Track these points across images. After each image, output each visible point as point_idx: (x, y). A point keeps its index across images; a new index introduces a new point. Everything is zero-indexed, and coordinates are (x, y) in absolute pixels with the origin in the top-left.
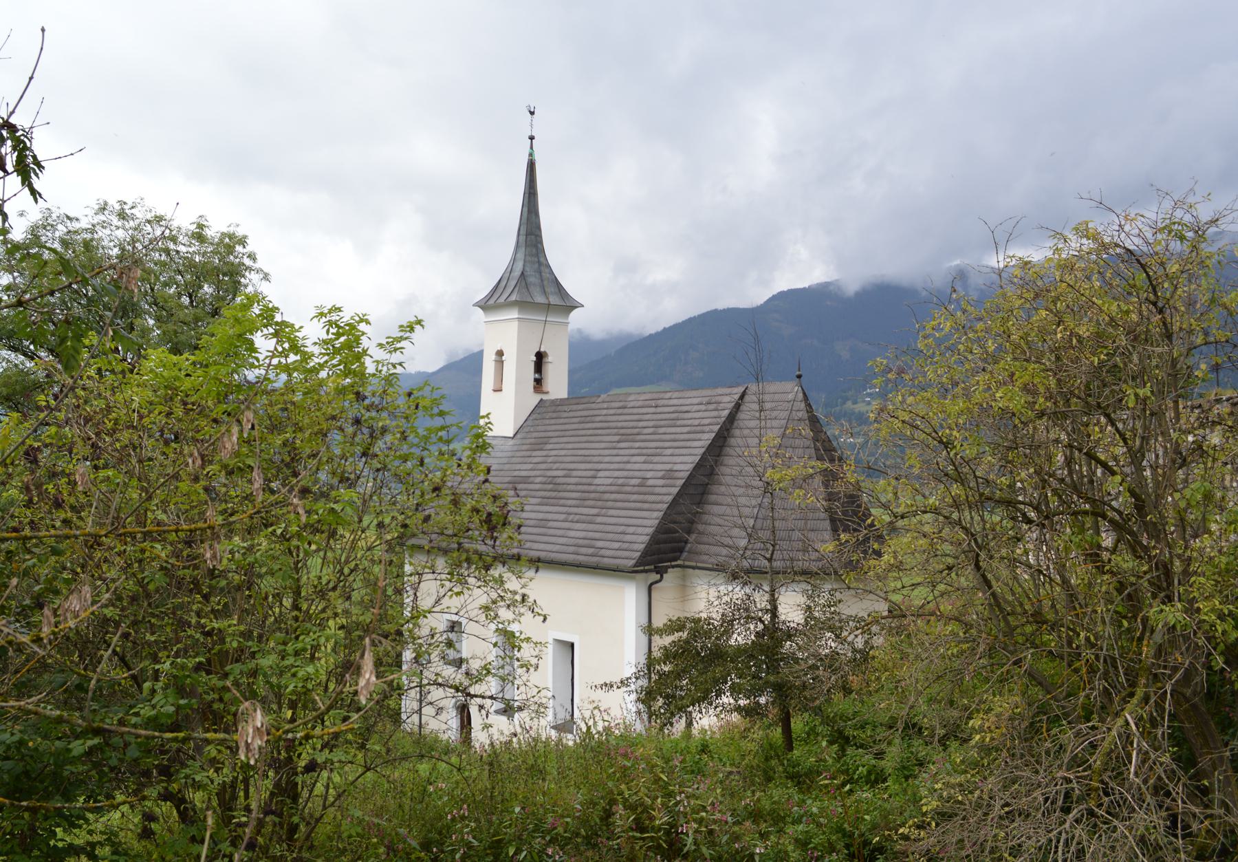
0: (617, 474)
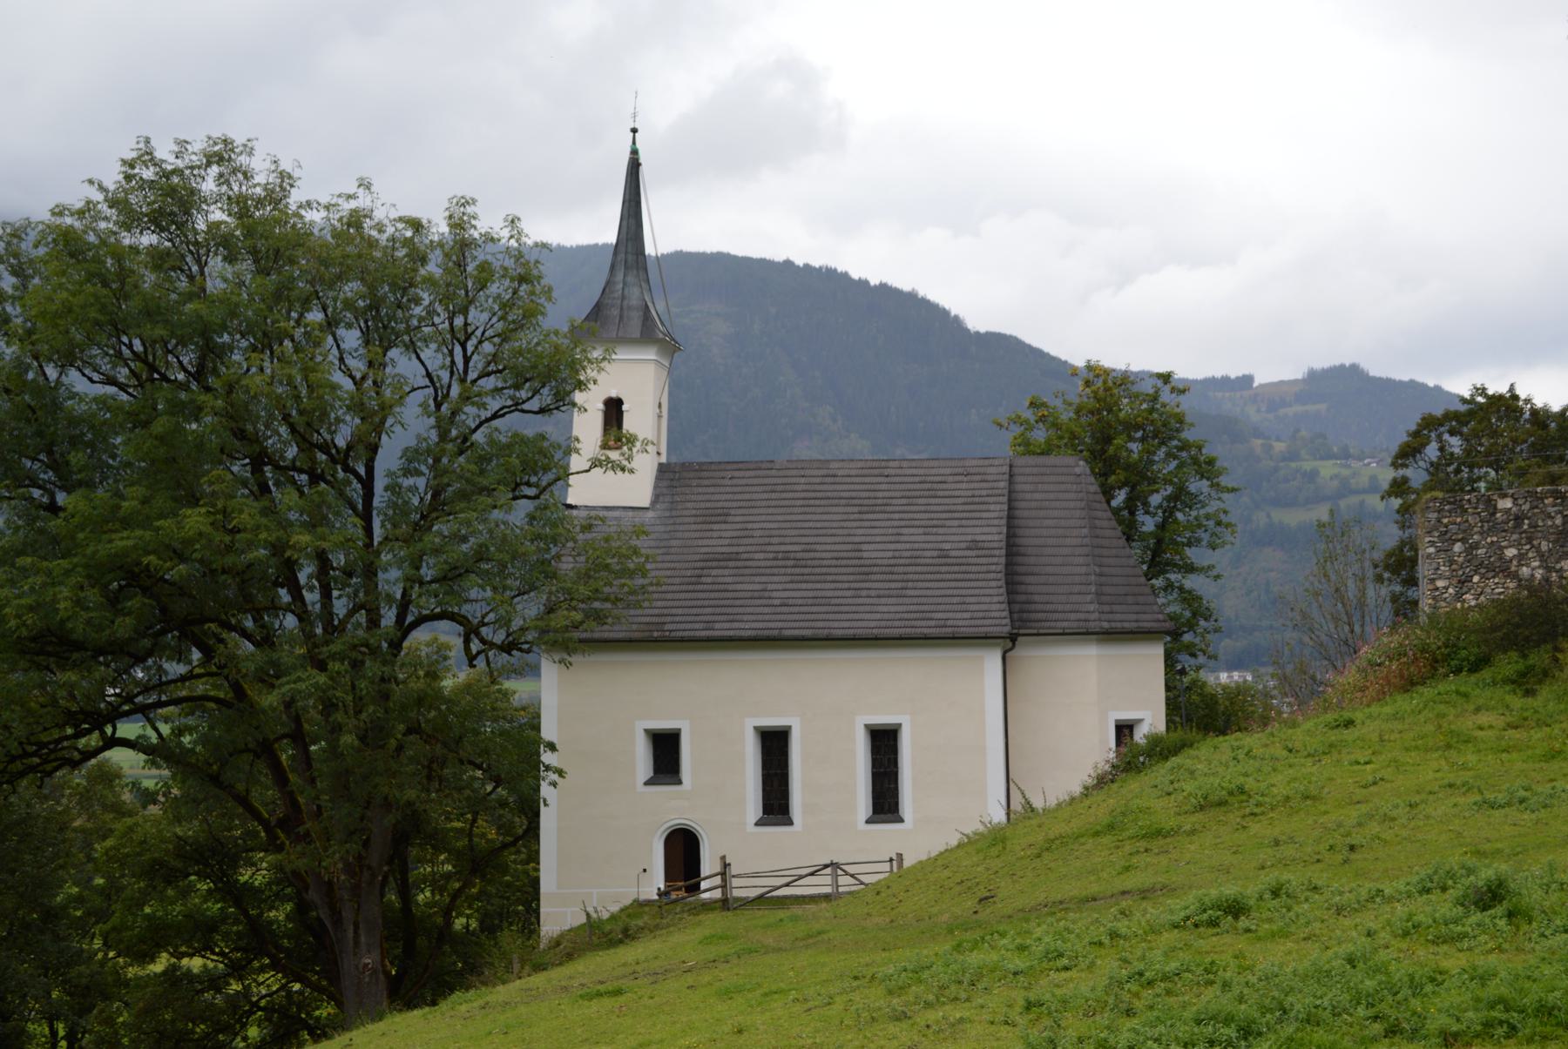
0: (893, 546)
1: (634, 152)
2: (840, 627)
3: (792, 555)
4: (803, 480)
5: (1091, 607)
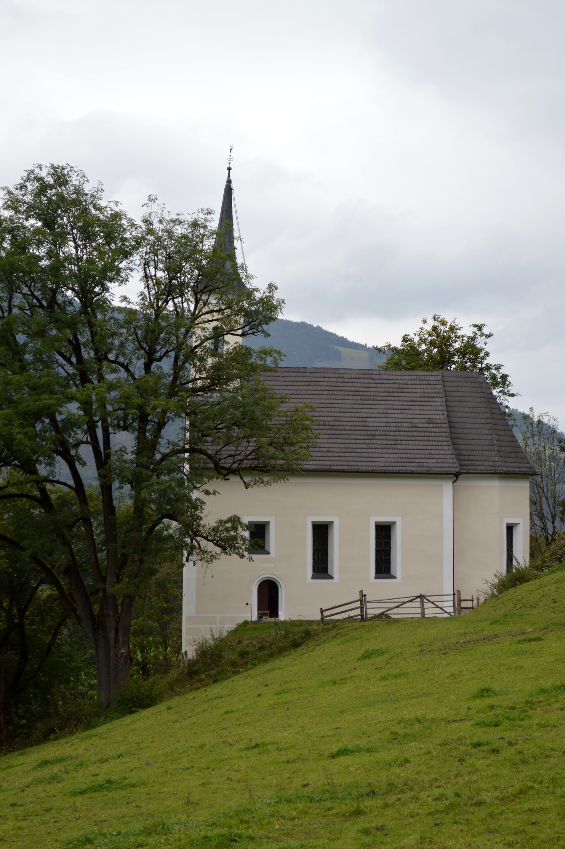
0: (384, 420)
1: (229, 181)
2: (364, 465)
3: (328, 423)
4: (325, 380)
5: (496, 459)
